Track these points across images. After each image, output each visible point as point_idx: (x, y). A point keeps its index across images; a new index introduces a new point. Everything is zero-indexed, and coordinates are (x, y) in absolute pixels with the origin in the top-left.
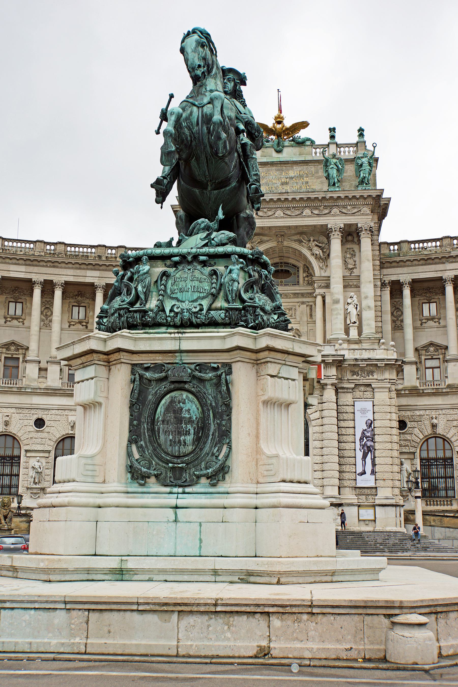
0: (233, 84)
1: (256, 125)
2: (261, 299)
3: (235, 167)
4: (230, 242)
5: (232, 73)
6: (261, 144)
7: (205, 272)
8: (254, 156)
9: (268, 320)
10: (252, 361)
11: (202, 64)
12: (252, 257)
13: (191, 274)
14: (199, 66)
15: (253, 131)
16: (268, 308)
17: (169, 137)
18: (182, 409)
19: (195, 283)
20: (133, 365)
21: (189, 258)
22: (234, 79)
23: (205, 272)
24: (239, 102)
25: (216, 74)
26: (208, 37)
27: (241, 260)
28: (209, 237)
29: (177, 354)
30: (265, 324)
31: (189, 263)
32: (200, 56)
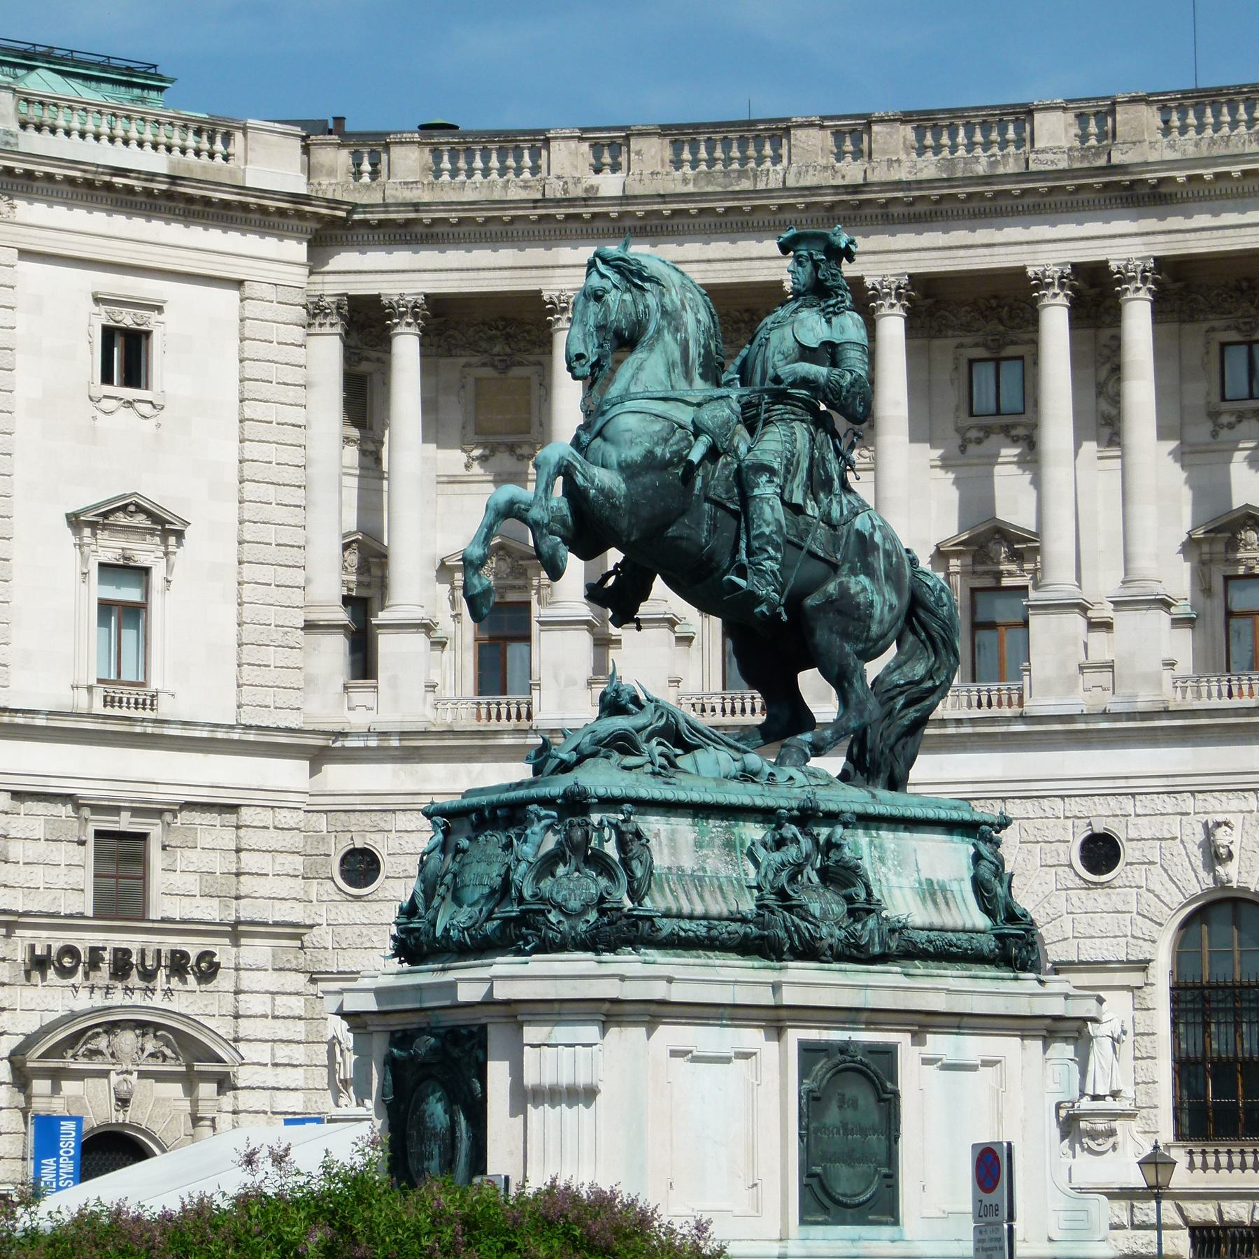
0: (809, 265)
1: (822, 380)
2: (575, 887)
3: (713, 529)
4: (604, 746)
6: (861, 409)
9: (572, 928)
10: (504, 1020)
14: (580, 357)
16: (574, 904)
18: (424, 1111)
20: (393, 1033)
22: (811, 255)
24: (823, 310)
25: (659, 331)
27: (543, 813)
29: (429, 1013)
30: (564, 938)
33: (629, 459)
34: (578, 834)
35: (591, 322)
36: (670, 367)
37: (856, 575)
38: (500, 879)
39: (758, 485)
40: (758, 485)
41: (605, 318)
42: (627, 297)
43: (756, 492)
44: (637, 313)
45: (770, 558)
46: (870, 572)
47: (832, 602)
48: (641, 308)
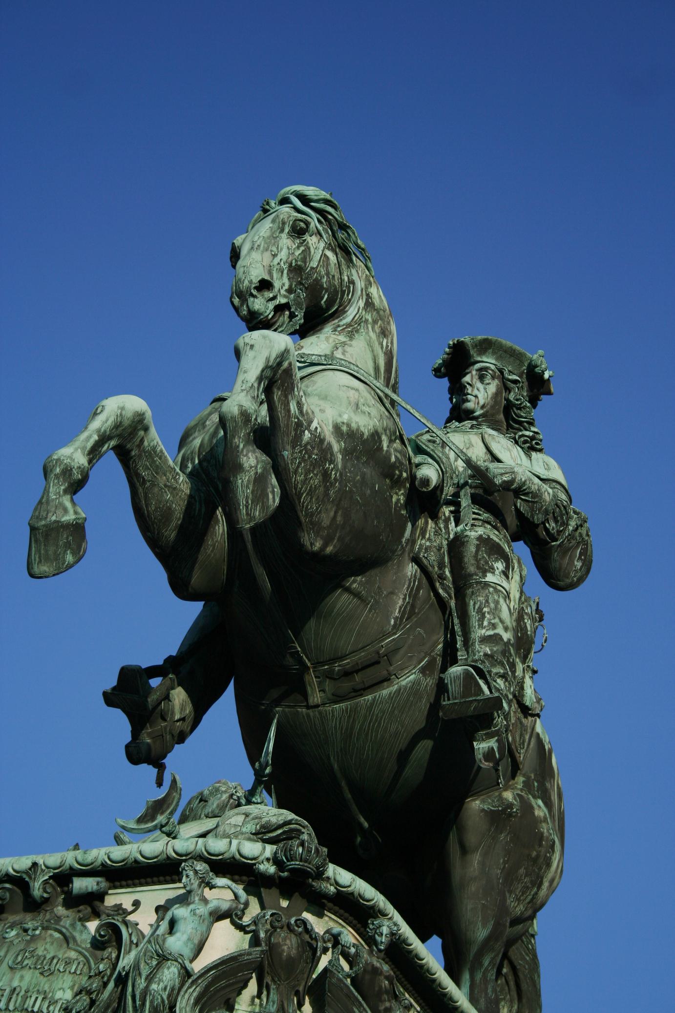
0: (493, 387)
3: (409, 612)
5: (494, 353)
6: (578, 564)
7: (84, 936)
8: (490, 578)
11: (281, 283)
12: (272, 869)
13: (22, 946)
14: (265, 285)
15: (538, 518)
17: (57, 476)
19: (22, 977)
21: (37, 889)
22: (501, 371)
23: (84, 936)
26: (329, 209)
28: (161, 819)
31: (33, 906)
32: (277, 260)
33: (354, 426)
34: (289, 945)
35: (283, 255)
36: (377, 369)
37: (535, 797)
38: (85, 999)
39: (492, 570)
40: (492, 570)
41: (304, 260)
42: (329, 254)
43: (490, 578)
44: (342, 280)
45: (504, 676)
46: (548, 804)
47: (510, 815)
48: (346, 279)
